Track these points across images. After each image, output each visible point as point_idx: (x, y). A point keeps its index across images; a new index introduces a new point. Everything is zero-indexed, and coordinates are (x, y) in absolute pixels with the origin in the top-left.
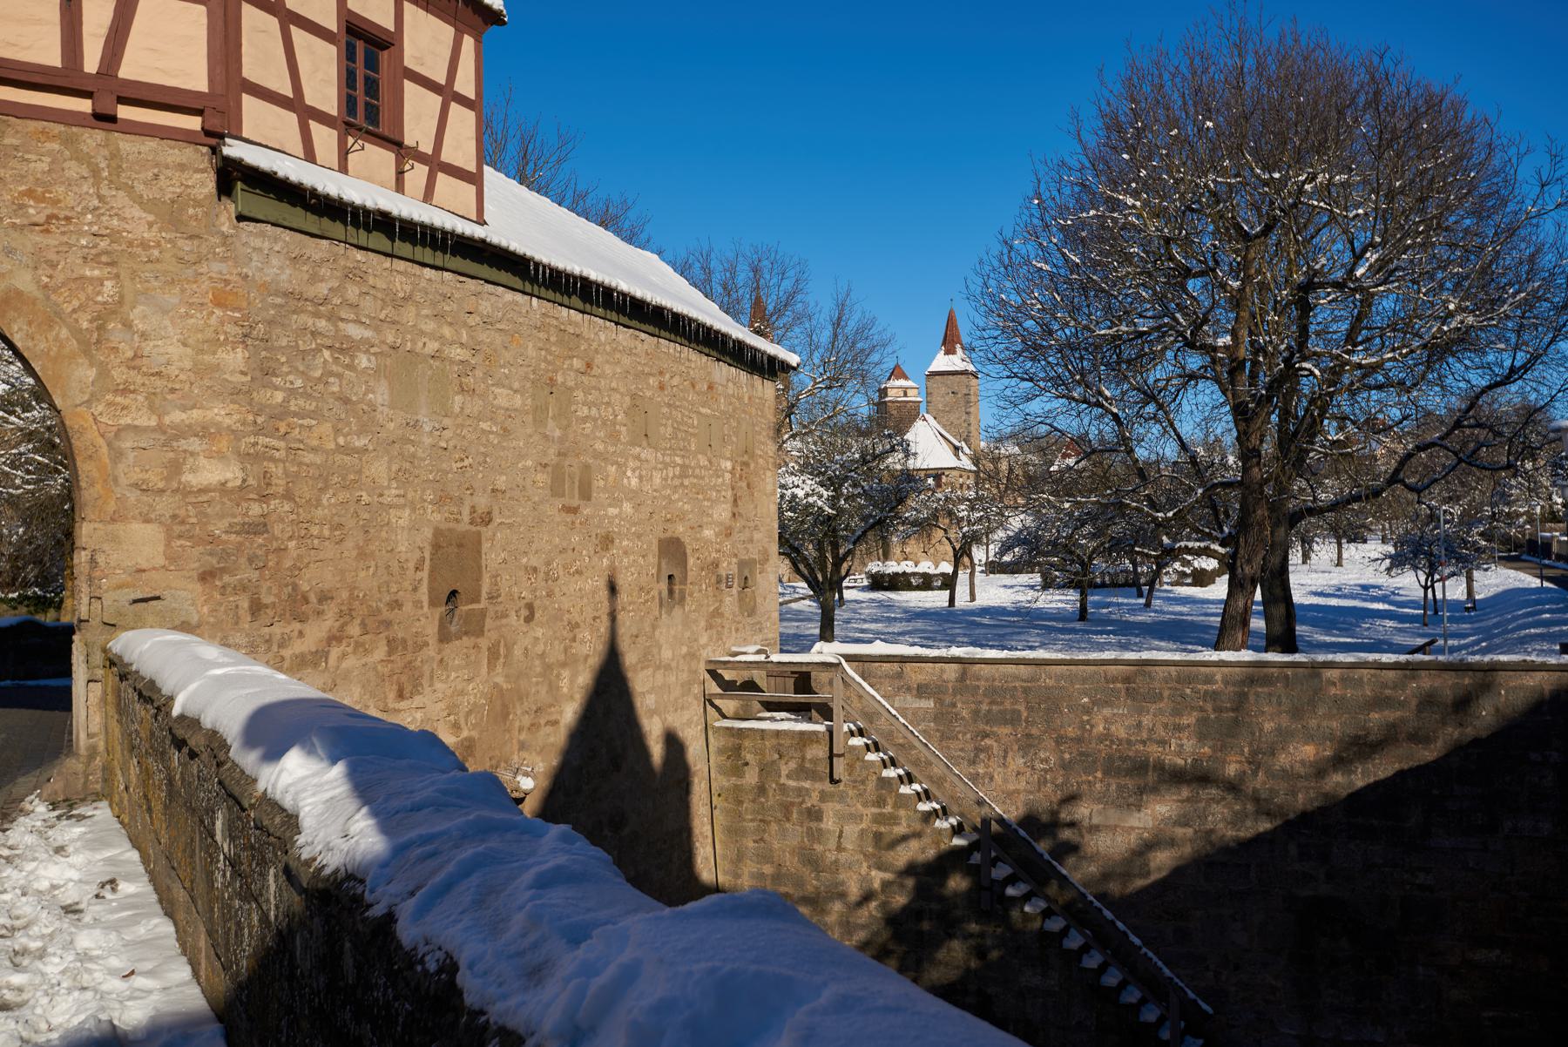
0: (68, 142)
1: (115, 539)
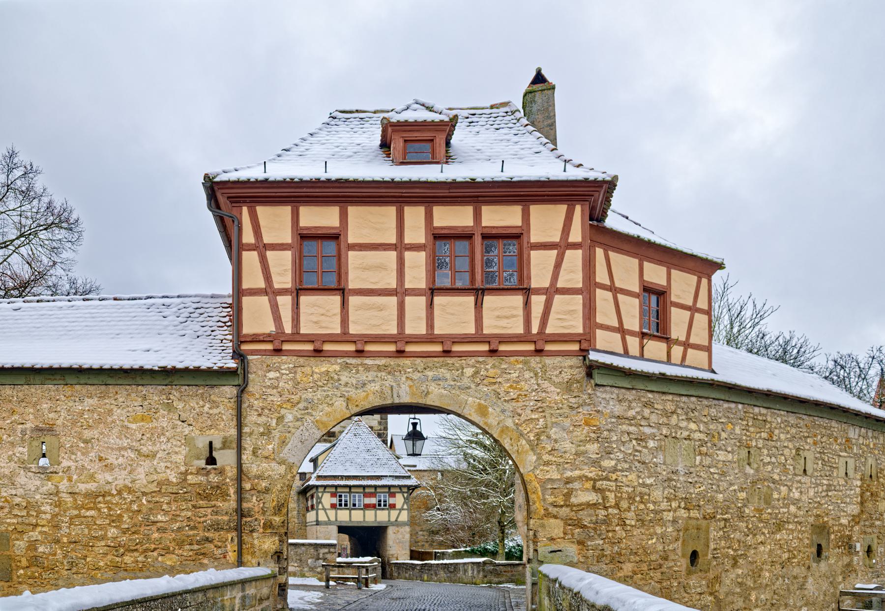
0: (525, 363)
1: (543, 526)
